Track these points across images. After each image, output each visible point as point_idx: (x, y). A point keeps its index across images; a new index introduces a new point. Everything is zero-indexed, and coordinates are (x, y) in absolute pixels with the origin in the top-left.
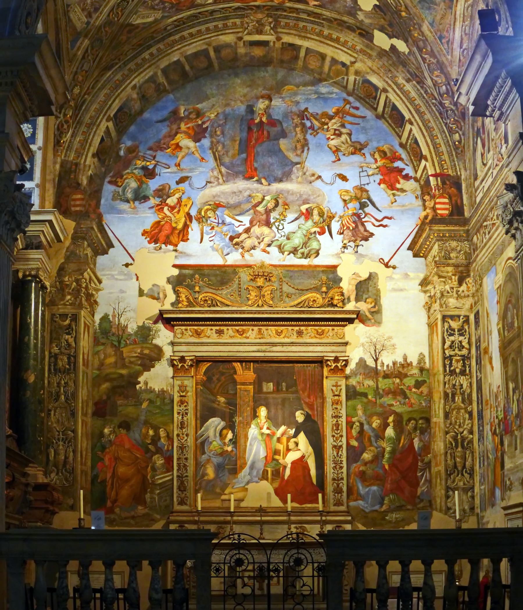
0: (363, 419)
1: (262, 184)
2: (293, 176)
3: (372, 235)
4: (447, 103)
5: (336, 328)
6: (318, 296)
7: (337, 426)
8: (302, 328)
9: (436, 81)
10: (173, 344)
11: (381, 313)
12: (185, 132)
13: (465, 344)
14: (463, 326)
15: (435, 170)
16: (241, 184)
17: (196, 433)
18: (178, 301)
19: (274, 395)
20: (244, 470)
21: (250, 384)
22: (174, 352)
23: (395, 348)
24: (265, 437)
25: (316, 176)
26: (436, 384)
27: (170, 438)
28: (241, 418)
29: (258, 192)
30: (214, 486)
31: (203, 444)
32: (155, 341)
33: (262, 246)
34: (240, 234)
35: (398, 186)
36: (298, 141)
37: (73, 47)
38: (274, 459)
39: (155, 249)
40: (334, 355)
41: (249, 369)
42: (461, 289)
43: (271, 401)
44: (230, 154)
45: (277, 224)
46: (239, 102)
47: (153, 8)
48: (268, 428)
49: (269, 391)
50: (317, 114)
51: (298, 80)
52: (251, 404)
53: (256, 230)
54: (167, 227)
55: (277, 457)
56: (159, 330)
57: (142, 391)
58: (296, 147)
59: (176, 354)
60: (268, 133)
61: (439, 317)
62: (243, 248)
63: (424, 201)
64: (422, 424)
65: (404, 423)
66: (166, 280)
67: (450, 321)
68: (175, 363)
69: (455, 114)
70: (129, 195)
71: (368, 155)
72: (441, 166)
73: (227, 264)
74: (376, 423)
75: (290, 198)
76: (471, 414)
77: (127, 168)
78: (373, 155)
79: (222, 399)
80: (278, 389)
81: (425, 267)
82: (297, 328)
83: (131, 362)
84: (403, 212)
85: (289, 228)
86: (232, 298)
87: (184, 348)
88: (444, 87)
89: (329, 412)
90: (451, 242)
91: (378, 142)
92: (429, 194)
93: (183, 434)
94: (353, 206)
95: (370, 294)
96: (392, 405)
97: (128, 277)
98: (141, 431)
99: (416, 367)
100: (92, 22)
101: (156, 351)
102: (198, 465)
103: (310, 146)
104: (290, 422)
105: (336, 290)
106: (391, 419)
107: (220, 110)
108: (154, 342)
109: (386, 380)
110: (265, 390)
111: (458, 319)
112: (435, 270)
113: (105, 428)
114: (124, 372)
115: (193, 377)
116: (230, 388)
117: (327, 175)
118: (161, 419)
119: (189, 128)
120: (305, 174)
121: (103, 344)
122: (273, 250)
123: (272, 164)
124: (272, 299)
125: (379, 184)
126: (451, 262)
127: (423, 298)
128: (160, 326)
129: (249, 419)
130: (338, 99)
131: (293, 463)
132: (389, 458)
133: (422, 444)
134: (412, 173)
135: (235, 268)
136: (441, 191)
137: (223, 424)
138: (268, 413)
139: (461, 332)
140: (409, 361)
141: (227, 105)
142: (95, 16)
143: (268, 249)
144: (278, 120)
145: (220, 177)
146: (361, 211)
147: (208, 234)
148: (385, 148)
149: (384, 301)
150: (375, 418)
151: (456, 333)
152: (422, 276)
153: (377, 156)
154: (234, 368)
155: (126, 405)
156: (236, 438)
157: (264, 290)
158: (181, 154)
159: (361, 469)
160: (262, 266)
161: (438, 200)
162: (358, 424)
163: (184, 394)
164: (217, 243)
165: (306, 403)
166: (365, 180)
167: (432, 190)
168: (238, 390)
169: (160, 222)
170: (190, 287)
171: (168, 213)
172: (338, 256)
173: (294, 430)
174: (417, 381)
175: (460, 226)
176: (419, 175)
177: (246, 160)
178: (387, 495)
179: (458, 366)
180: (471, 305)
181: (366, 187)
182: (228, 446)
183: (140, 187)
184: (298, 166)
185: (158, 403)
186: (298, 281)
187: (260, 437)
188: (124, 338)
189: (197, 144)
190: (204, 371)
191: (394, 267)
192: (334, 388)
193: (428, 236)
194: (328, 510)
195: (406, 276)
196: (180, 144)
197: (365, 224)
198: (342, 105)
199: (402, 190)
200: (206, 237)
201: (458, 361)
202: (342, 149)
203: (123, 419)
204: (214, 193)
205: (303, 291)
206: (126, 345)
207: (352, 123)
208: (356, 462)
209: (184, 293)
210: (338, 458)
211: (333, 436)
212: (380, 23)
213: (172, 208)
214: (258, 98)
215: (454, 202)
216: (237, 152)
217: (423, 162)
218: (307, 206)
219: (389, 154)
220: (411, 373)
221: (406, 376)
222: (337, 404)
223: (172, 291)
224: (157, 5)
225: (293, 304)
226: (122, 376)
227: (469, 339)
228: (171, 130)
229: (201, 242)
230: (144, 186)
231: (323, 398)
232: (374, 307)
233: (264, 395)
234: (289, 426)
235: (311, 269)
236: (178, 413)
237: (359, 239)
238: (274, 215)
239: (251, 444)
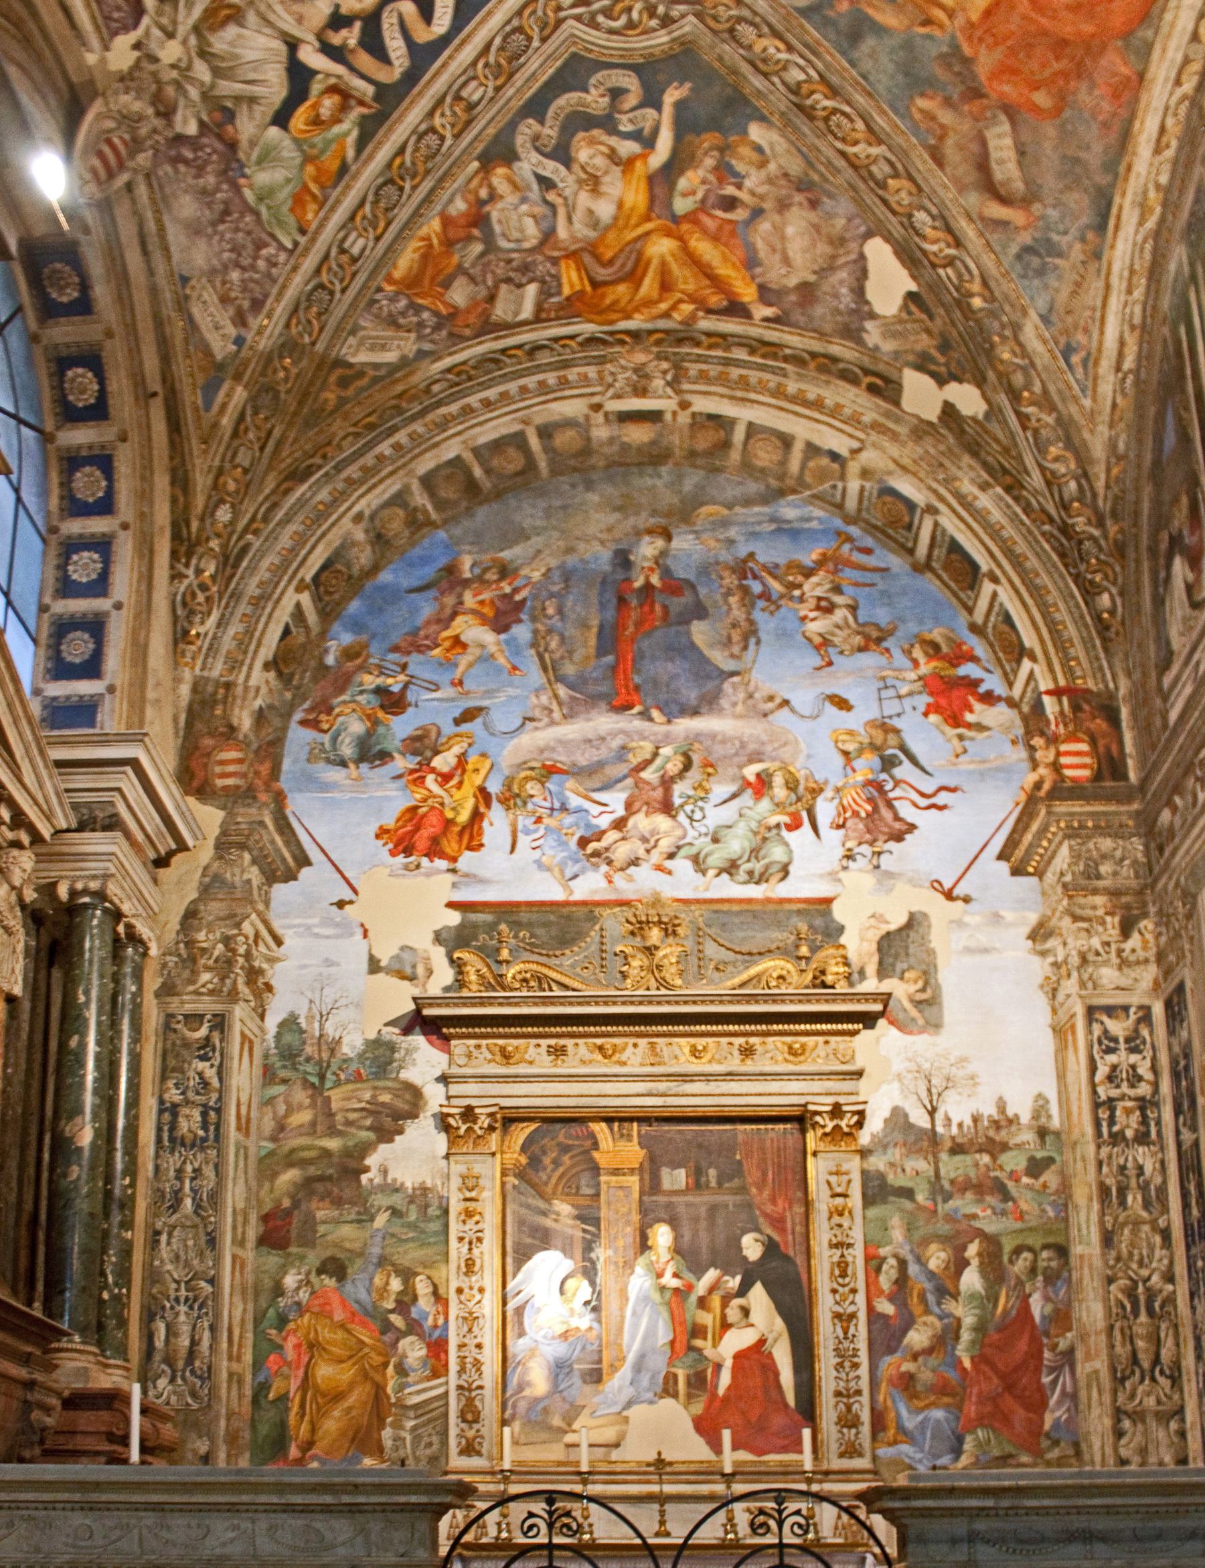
0: (905, 1252)
1: (651, 719)
2: (724, 703)
3: (912, 827)
4: (1080, 523)
5: (833, 1039)
6: (789, 966)
7: (843, 1268)
8: (752, 1040)
9: (1053, 473)
10: (444, 1079)
11: (940, 1005)
12: (474, 612)
13: (1144, 1070)
14: (1136, 1031)
15: (1055, 680)
16: (604, 722)
18: (460, 983)
19: (689, 1198)
20: (618, 1375)
22: (448, 1098)
23: (976, 1084)
24: (668, 1295)
25: (778, 701)
26: (1079, 1165)
28: (610, 1252)
29: (644, 739)
30: (545, 1411)
31: (519, 1311)
32: (407, 1075)
33: (655, 857)
34: (604, 832)
35: (969, 718)
36: (734, 626)
37: (208, 406)
38: (691, 1348)
39: (406, 867)
40: (831, 1100)
41: (629, 1138)
42: (1128, 945)
43: (682, 1210)
44: (577, 657)
45: (688, 808)
46: (595, 543)
47: (392, 322)
48: (675, 1275)
50: (777, 566)
51: (731, 493)
52: (636, 1217)
53: (641, 822)
54: (434, 819)
55: (698, 1343)
56: (416, 1049)
58: (729, 638)
59: (454, 1102)
60: (665, 608)
61: (1080, 1010)
62: (610, 863)
63: (1032, 749)
66: (431, 936)
67: (1105, 1019)
68: (452, 1121)
69: (1101, 549)
70: (347, 750)
71: (896, 652)
72: (1069, 672)
73: (573, 898)
74: (937, 1258)
75: (719, 750)
76: (1166, 1234)
77: (341, 690)
78: (908, 652)
79: (564, 1208)
80: (697, 1183)
81: (1039, 898)
82: (742, 1040)
83: (349, 1123)
84: (982, 775)
85: (715, 816)
86: (585, 973)
87: (472, 1088)
88: (1073, 485)
89: (822, 1235)
90: (1100, 840)
91: (921, 622)
92: (1042, 734)
94: (866, 765)
95: (912, 960)
96: (974, 1217)
97: (345, 930)
99: (1030, 1127)
100: (249, 337)
101: (408, 1097)
103: (763, 636)
104: (729, 1258)
105: (832, 951)
106: (972, 1250)
107: (553, 563)
108: (404, 1075)
109: (958, 1158)
110: (666, 1184)
111: (1122, 1015)
112: (1065, 902)
114: (333, 1144)
116: (583, 1182)
117: (804, 697)
119: (482, 603)
120: (751, 696)
121: (285, 1081)
122: (682, 866)
123: (675, 677)
124: (681, 973)
125: (926, 714)
126: (1101, 884)
127: (1039, 968)
128: (418, 1040)
129: (631, 1253)
130: (824, 532)
131: (739, 1356)
132: (973, 1342)
133: (1049, 1308)
134: (1000, 689)
135: (590, 909)
136: (1071, 727)
137: (568, 1265)
138: (675, 1239)
139: (1134, 1043)
140: (1010, 1112)
141: (570, 550)
142: (255, 322)
143: (669, 864)
144: (687, 581)
145: (555, 707)
146: (884, 776)
147: (527, 832)
148: (937, 635)
149: (946, 977)
150: (933, 1247)
151: (1122, 1046)
152: (1033, 918)
153: (918, 653)
154: (592, 1136)
157: (661, 953)
158: (464, 661)
159: (904, 1368)
160: (656, 902)
161: (1064, 748)
162: (892, 1261)
163: (473, 1194)
164: (550, 852)
165: (766, 1216)
166: (891, 707)
167: (1048, 722)
168: (604, 1187)
169: (416, 808)
170: (490, 954)
171: (436, 789)
172: (833, 877)
173: (738, 1278)
174: (1032, 1160)
175: (1119, 802)
176: (1016, 692)
177: (614, 668)
178: (972, 1431)
179: (1129, 1124)
180: (1156, 983)
181: (896, 723)
182: (581, 1316)
183: (370, 733)
184: (736, 679)
185: (413, 1216)
186: (741, 934)
187: (656, 1296)
188: (334, 1067)
189: (503, 637)
190: (520, 1142)
191: (967, 900)
192: (833, 1179)
193: (1044, 829)
194: (825, 1467)
195: (996, 918)
196: (463, 638)
197: (896, 803)
198: (834, 544)
199: (980, 727)
200: (524, 841)
201: (1128, 1112)
202: (836, 640)
204: (541, 743)
205: (752, 956)
206: (338, 1083)
207: (857, 584)
208: (891, 1351)
209: (474, 964)
210: (846, 1344)
211: (834, 1291)
212: (918, 347)
213: (445, 778)
214: (638, 534)
215: (1101, 749)
216: (592, 651)
217: (1026, 665)
218: (756, 768)
219: (945, 649)
220: (1018, 1139)
221: (1005, 1147)
222: (841, 1214)
223: (445, 961)
224: (403, 314)
225: (729, 984)
226: (326, 1153)
227: (1154, 1059)
228: (442, 608)
229: (512, 851)
230: (381, 730)
231: (807, 1204)
232: (923, 990)
234: (727, 1270)
235: (771, 907)
236: (461, 1239)
237: (882, 838)
238: (680, 790)
239: (634, 1313)
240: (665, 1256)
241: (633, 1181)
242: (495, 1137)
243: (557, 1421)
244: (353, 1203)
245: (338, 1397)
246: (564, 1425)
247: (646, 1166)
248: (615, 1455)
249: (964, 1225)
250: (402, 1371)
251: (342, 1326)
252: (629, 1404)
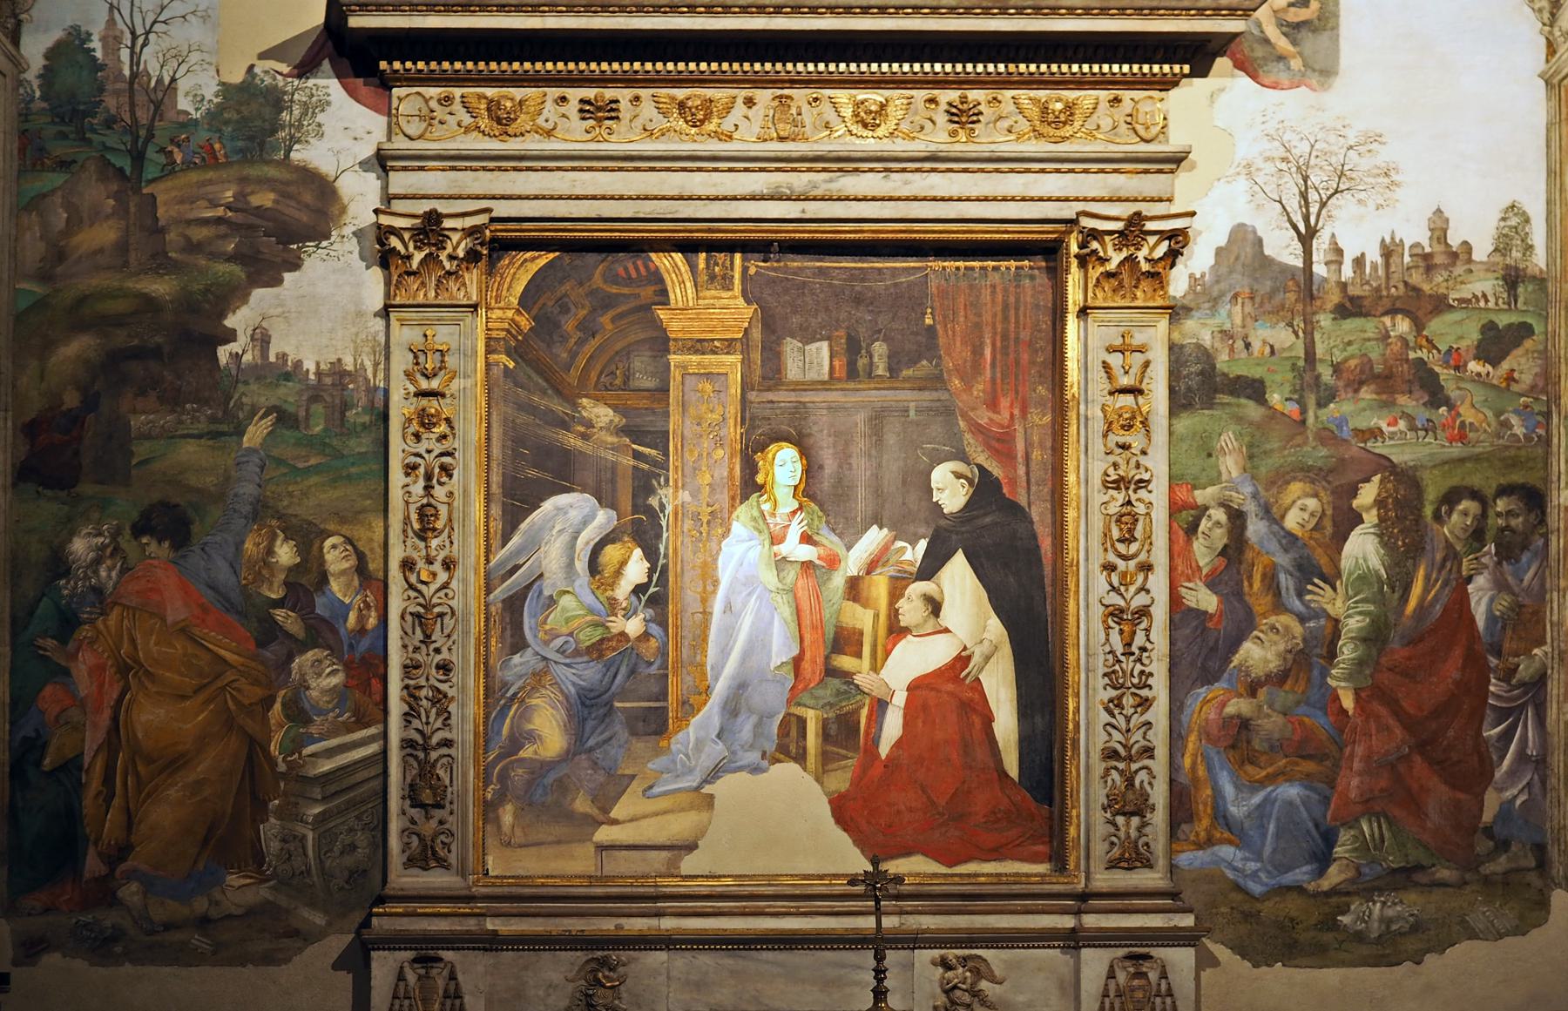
0: (1242, 497)
17: (488, 560)
21: (729, 346)
22: (388, 198)
24: (791, 574)
27: (370, 578)
38: (831, 672)
41: (727, 284)
48: (806, 539)
49: (812, 375)
55: (845, 662)
57: (240, 374)
59: (398, 206)
64: (1509, 513)
65: (1428, 511)
68: (394, 242)
87: (434, 181)
93: (430, 562)
96: (1376, 433)
98: (239, 545)
102: (497, 698)
106: (1367, 494)
110: (793, 371)
113: (72, 533)
115: (475, 307)
118: (329, 496)
150: (1296, 488)
155: (171, 436)
156: (663, 580)
163: (435, 384)
173: (922, 545)
187: (769, 577)
203: (156, 496)
226: (149, 304)
233: (792, 397)
236: (410, 469)
239: (728, 608)
240: (787, 503)
241: (731, 363)
242: (473, 278)
243: (582, 804)
244: (205, 402)
245: (176, 763)
246: (595, 812)
247: (756, 334)
248: (689, 864)
249: (1354, 449)
250: (298, 713)
251: (184, 631)
252: (714, 775)
